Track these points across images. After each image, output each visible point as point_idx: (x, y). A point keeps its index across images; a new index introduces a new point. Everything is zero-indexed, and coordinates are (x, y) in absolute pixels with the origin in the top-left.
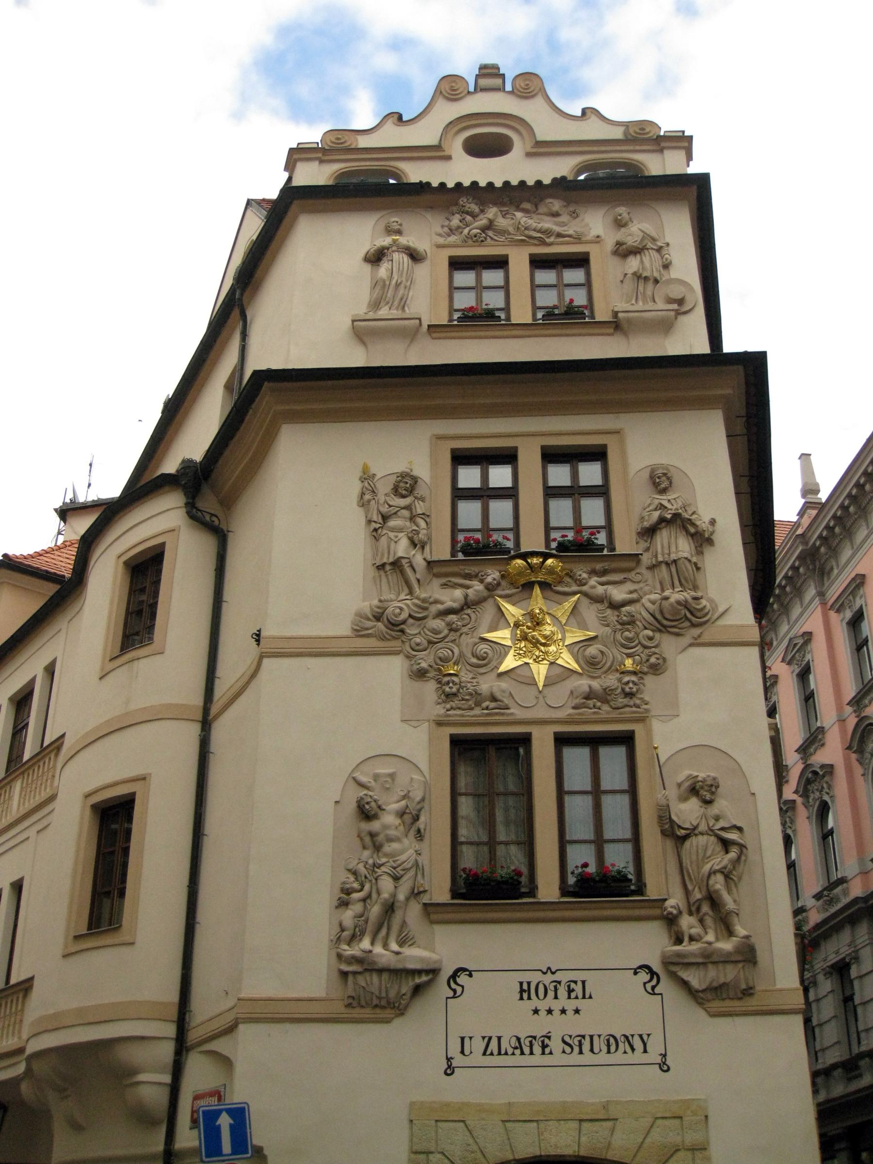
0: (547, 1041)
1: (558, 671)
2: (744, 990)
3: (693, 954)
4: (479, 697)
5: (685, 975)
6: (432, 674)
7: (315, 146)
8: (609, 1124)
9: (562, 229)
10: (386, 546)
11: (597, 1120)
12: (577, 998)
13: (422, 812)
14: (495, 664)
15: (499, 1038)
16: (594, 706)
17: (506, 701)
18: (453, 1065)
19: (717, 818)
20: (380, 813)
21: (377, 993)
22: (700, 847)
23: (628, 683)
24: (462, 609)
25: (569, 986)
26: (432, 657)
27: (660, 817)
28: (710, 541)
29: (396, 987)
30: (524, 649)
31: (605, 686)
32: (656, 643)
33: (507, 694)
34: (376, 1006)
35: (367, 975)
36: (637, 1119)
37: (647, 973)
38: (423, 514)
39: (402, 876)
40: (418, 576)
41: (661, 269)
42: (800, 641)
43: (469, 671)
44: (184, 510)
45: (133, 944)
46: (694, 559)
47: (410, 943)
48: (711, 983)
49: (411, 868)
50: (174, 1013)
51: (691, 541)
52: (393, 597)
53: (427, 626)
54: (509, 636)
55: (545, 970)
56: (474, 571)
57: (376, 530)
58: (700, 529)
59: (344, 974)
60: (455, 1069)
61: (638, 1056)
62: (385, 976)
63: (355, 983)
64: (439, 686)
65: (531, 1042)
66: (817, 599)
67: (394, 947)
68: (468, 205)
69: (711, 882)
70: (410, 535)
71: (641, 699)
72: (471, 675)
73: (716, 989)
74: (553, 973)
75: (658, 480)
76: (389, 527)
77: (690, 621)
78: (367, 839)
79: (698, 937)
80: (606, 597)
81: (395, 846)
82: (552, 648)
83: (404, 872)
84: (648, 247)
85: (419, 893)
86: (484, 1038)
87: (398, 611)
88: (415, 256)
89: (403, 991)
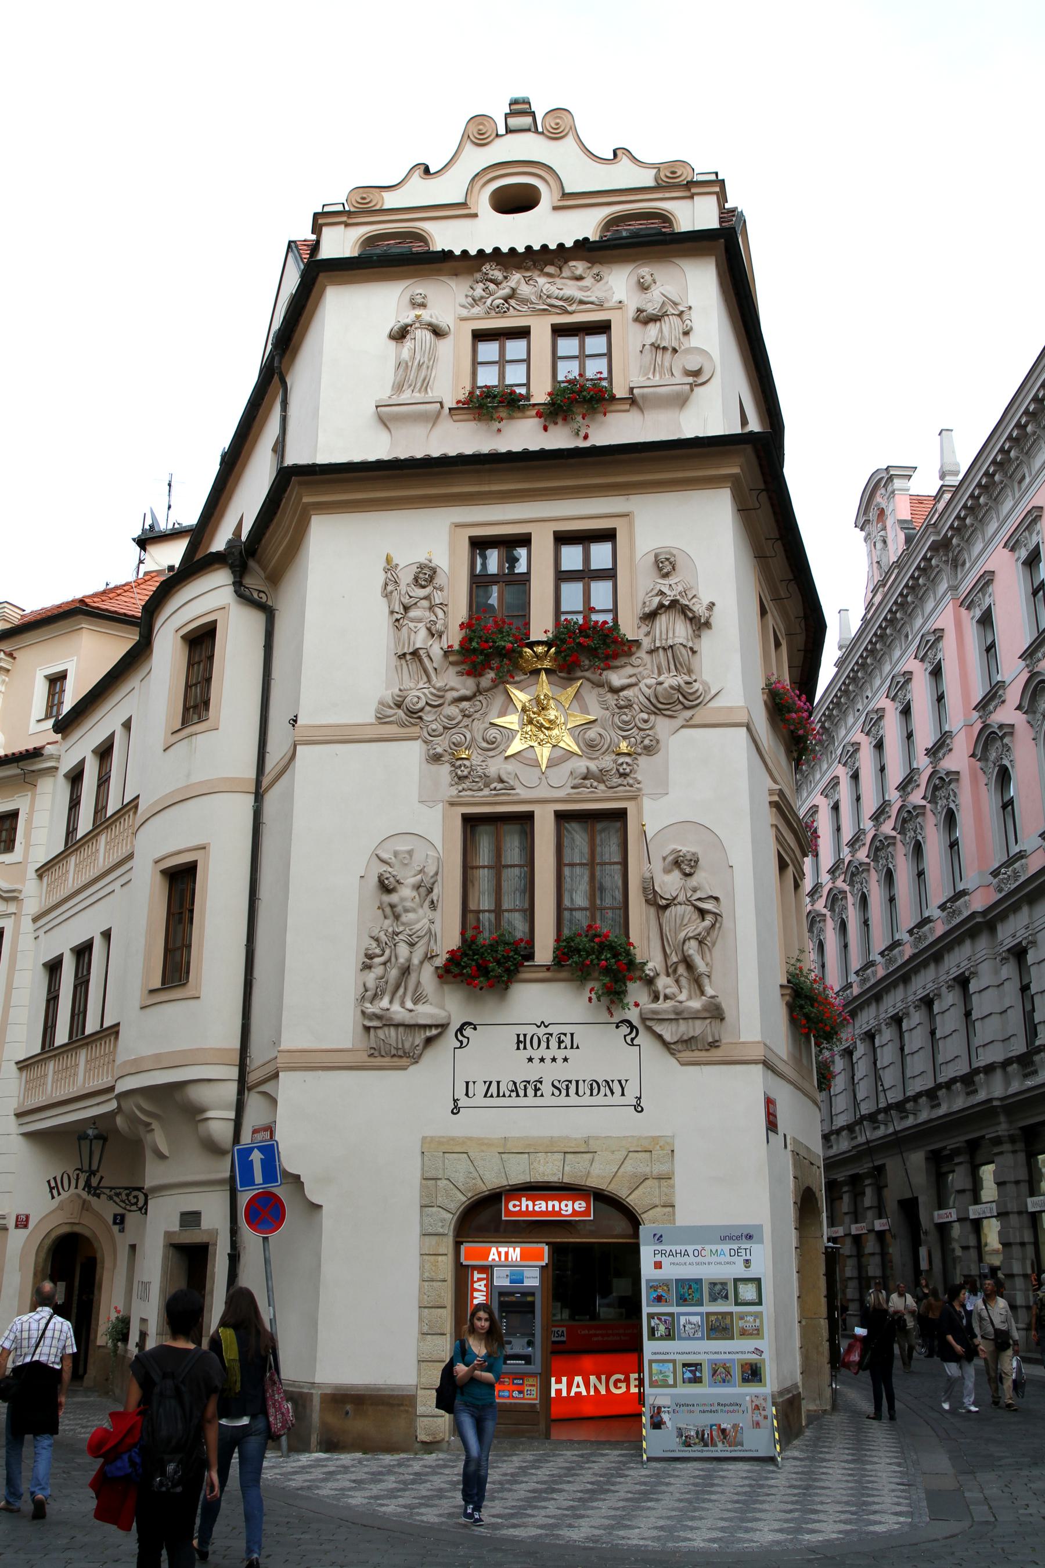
0: (539, 1085)
1: (563, 752)
3: (665, 1011)
5: (659, 1029)
6: (446, 758)
7: (340, 208)
9: (586, 294)
12: (566, 1048)
13: (436, 885)
15: (498, 1083)
17: (512, 783)
19: (695, 890)
20: (398, 886)
22: (678, 916)
23: (622, 763)
24: (474, 695)
25: (559, 1038)
27: (645, 889)
28: (707, 624)
29: (411, 1039)
34: (394, 1056)
35: (386, 1029)
36: (613, 1152)
38: (441, 604)
40: (435, 665)
41: (681, 336)
42: (933, 638)
44: (231, 588)
46: (690, 644)
48: (681, 1037)
50: (236, 1058)
51: (689, 625)
52: (412, 685)
57: (397, 620)
59: (367, 1029)
61: (617, 1099)
62: (401, 1029)
63: (376, 1036)
64: (453, 769)
65: (525, 1086)
66: (949, 593)
67: (409, 1005)
68: (491, 272)
69: (685, 948)
70: (428, 625)
72: (482, 759)
73: (686, 1041)
77: (682, 704)
78: (388, 910)
81: (411, 916)
82: (555, 732)
84: (668, 313)
86: (485, 1082)
87: (416, 699)
88: (437, 332)
89: (417, 1043)
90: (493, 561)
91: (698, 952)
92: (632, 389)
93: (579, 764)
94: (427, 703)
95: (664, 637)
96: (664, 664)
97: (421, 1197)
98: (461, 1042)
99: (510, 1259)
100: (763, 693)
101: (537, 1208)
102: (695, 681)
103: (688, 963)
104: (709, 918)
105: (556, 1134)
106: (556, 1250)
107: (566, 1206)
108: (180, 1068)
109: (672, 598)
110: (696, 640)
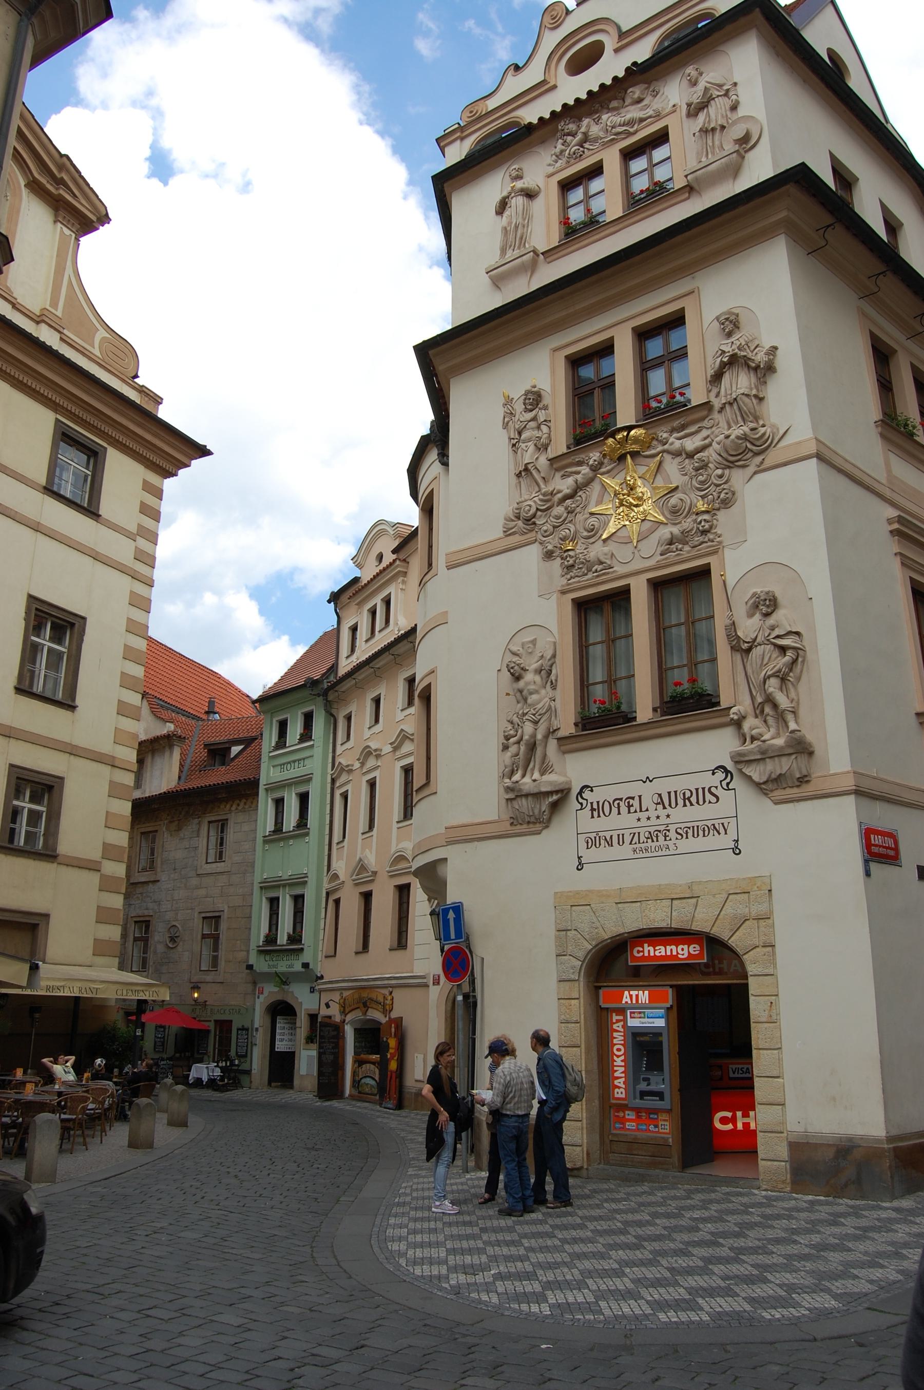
2: (799, 778)
3: (751, 752)
5: (747, 771)
8: (694, 900)
11: (684, 898)
17: (609, 562)
19: (772, 628)
23: (701, 522)
28: (770, 368)
29: (538, 806)
33: (609, 556)
34: (529, 823)
35: (519, 799)
36: (714, 895)
40: (542, 475)
41: (729, 113)
45: (436, 793)
46: (754, 392)
48: (770, 776)
49: (545, 713)
51: (752, 375)
52: (527, 497)
54: (611, 506)
57: (514, 445)
59: (507, 800)
62: (530, 798)
67: (536, 775)
68: (567, 127)
72: (585, 546)
74: (651, 781)
75: (722, 327)
77: (752, 451)
78: (518, 694)
84: (714, 96)
85: (555, 731)
87: (528, 508)
88: (530, 195)
89: (543, 809)
90: (587, 372)
91: (781, 690)
92: (686, 176)
95: (729, 392)
97: (556, 946)
98: (581, 804)
99: (640, 1002)
100: (877, 426)
101: (657, 953)
102: (763, 426)
103: (770, 700)
104: (789, 653)
106: (679, 991)
107: (683, 949)
108: (430, 852)
110: (763, 387)
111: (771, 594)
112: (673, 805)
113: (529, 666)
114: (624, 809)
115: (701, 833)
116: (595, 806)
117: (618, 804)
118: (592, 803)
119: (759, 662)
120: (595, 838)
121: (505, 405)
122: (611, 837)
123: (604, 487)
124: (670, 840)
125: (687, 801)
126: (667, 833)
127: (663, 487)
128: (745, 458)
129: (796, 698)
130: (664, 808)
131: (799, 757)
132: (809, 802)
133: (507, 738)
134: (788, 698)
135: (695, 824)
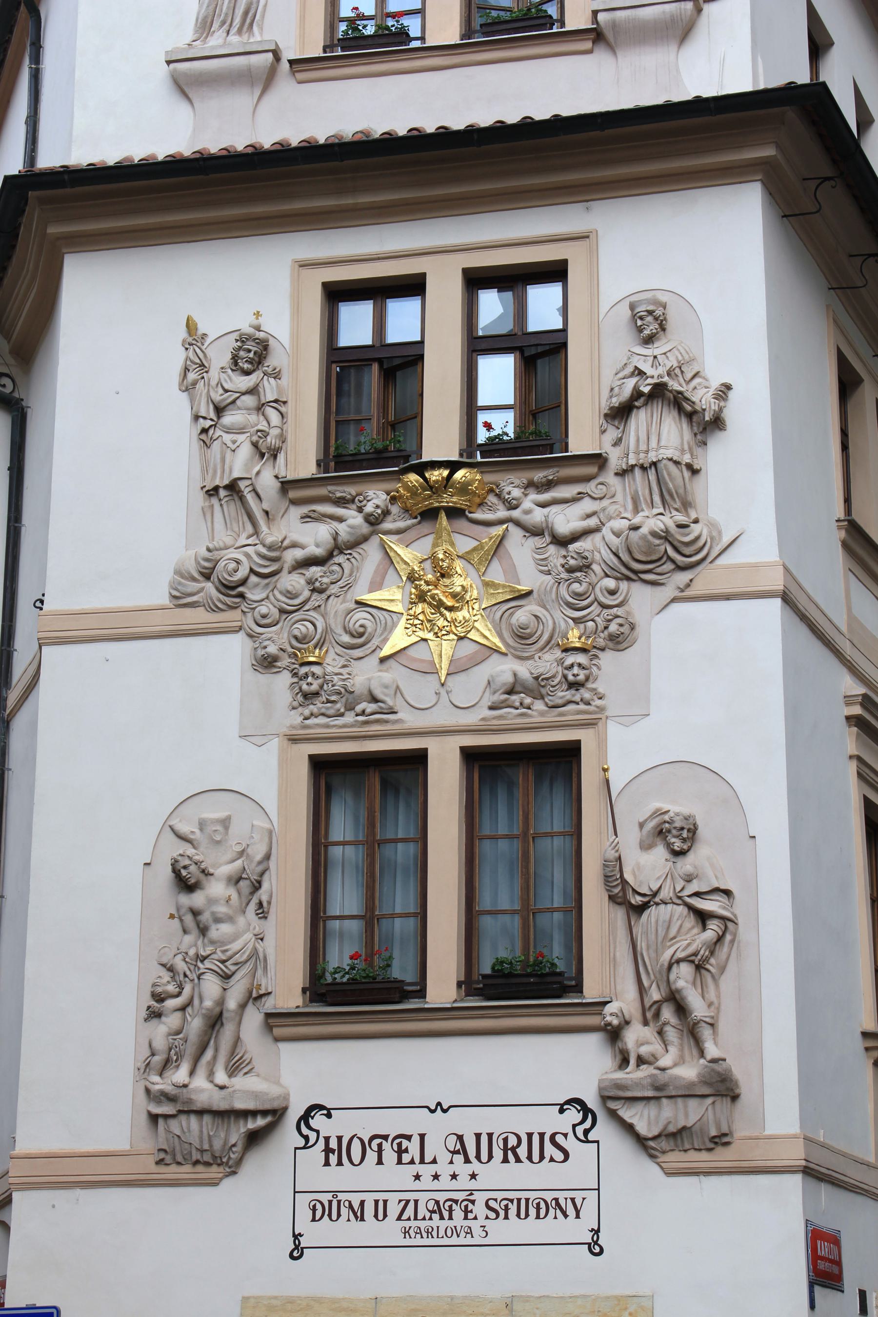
3: (638, 1084)
4: (351, 696)
5: (627, 1114)
6: (285, 661)
10: (218, 461)
13: (266, 877)
14: (377, 643)
16: (521, 704)
17: (390, 702)
18: (302, 1246)
19: (689, 879)
21: (196, 1143)
22: (660, 923)
23: (572, 666)
24: (330, 556)
26: (286, 635)
27: (607, 878)
28: (717, 423)
29: (223, 1135)
30: (421, 617)
31: (536, 672)
32: (621, 599)
34: (197, 1162)
35: (183, 1118)
37: (579, 1111)
38: (276, 401)
39: (234, 973)
40: (266, 506)
43: (339, 655)
46: (687, 458)
47: (245, 1070)
52: (229, 541)
53: (278, 586)
55: (433, 1108)
56: (351, 494)
57: (205, 431)
58: (698, 408)
59: (154, 1118)
60: (304, 1250)
62: (207, 1119)
63: (168, 1131)
64: (295, 680)
67: (221, 1077)
69: (672, 977)
70: (255, 438)
71: (594, 690)
72: (342, 662)
73: (673, 1135)
74: (445, 1111)
75: (639, 323)
76: (224, 426)
77: (673, 561)
78: (189, 919)
79: (651, 1059)
80: (547, 527)
81: (225, 929)
83: (236, 967)
85: (260, 997)
87: (233, 565)
89: (233, 1141)
91: (694, 984)
92: (595, 13)
93: (499, 668)
94: (252, 570)
95: (643, 447)
96: (643, 492)
98: (306, 1138)
100: (839, 528)
102: (696, 521)
104: (714, 926)
105: (459, 1292)
109: (655, 381)
110: (700, 450)
111: (691, 820)
112: (484, 1156)
113: (217, 866)
114: (390, 1155)
115: (532, 1212)
116: (333, 1144)
117: (380, 1146)
118: (327, 1139)
119: (661, 933)
120: (330, 1202)
121: (187, 345)
122: (362, 1203)
123: (388, 558)
124: (475, 1218)
125: (509, 1152)
126: (470, 1207)
127: (504, 586)
128: (659, 570)
129: (716, 1001)
130: (467, 1161)
131: (718, 1105)
132: (726, 1179)
133: (160, 998)
134: (703, 997)
135: (523, 1195)
